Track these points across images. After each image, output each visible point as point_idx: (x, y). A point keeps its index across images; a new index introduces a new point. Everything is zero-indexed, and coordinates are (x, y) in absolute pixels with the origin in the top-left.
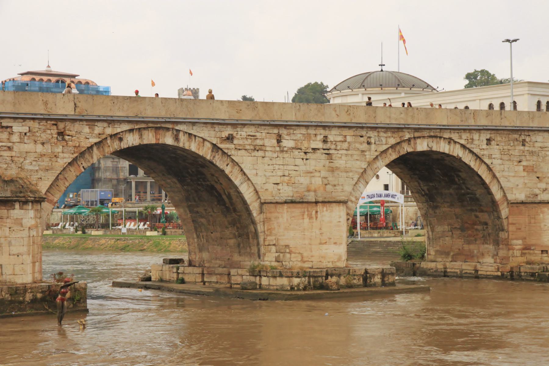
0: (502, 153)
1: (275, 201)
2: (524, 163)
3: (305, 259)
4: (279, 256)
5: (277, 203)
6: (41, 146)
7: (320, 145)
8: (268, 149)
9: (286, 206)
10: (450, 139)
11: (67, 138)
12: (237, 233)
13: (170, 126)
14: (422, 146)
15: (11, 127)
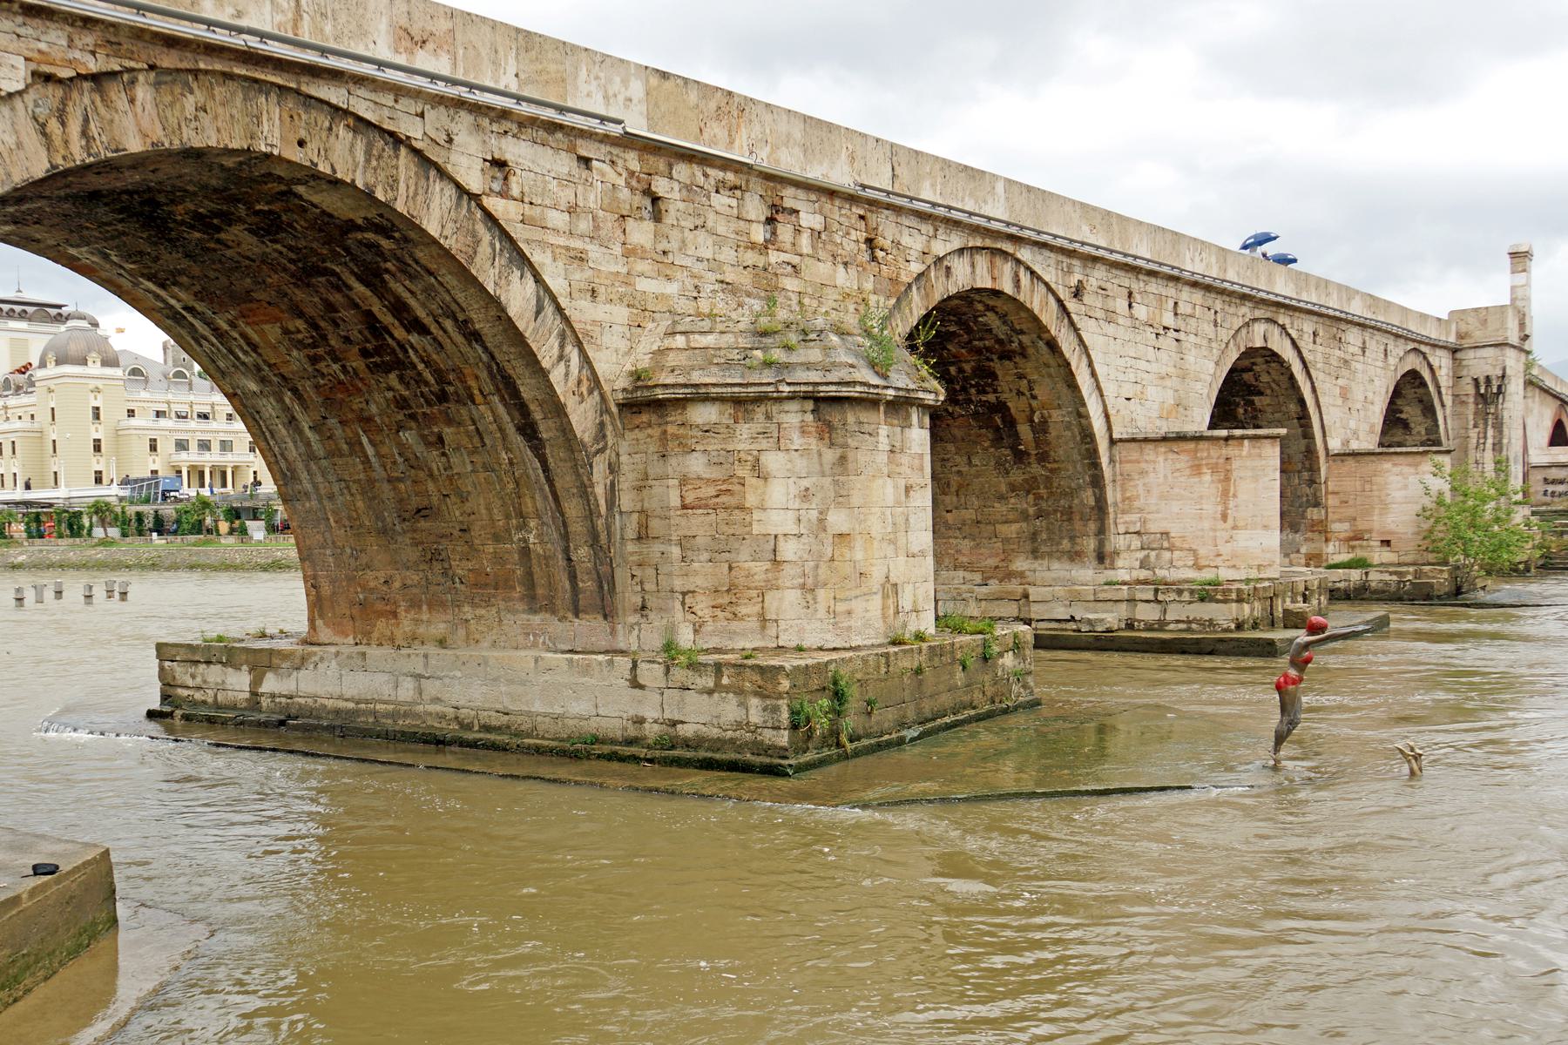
0: (1327, 358)
1: (1141, 436)
2: (1340, 382)
3: (1203, 562)
4: (1148, 556)
5: (1146, 440)
6: (841, 268)
7: (1168, 319)
8: (1121, 321)
9: (1162, 448)
10: (1283, 327)
11: (880, 254)
12: (1031, 511)
13: (1008, 247)
14: (1258, 336)
15: (798, 212)
